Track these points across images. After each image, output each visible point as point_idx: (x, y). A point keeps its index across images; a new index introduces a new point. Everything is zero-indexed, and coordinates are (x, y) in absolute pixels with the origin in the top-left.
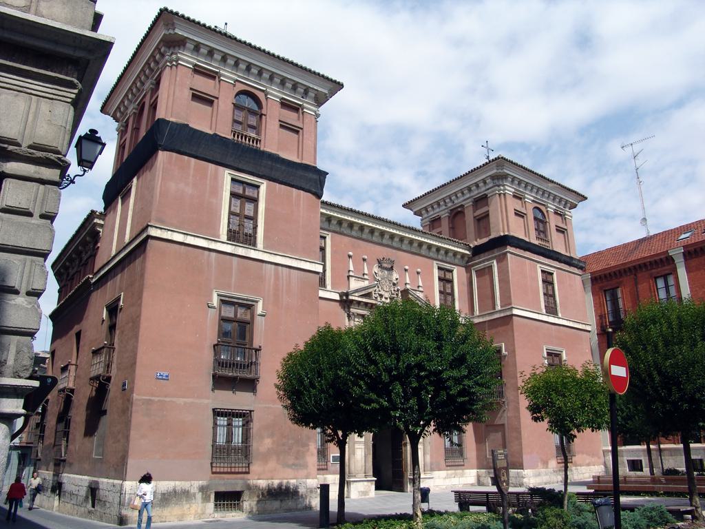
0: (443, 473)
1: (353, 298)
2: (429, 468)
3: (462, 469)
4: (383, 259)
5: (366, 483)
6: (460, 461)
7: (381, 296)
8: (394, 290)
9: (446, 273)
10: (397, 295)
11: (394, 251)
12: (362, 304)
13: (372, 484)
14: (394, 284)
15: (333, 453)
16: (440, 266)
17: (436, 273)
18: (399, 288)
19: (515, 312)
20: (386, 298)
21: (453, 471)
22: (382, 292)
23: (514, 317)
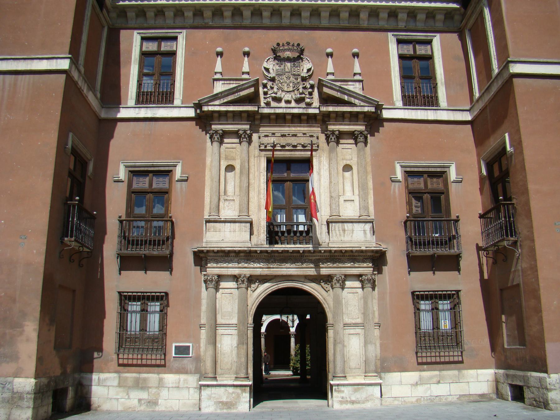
0: (412, 376)
1: (211, 108)
2: (372, 367)
3: (459, 369)
4: (278, 44)
5: (231, 390)
6: (454, 355)
7: (278, 100)
8: (305, 88)
9: (417, 46)
10: (311, 94)
11: (306, 32)
12: (229, 115)
13: (245, 391)
14: (304, 79)
15: (176, 342)
16: (401, 37)
17: (393, 50)
18: (311, 82)
19: (516, 69)
20: (288, 102)
21: (437, 373)
22: (280, 94)
23: (515, 80)
